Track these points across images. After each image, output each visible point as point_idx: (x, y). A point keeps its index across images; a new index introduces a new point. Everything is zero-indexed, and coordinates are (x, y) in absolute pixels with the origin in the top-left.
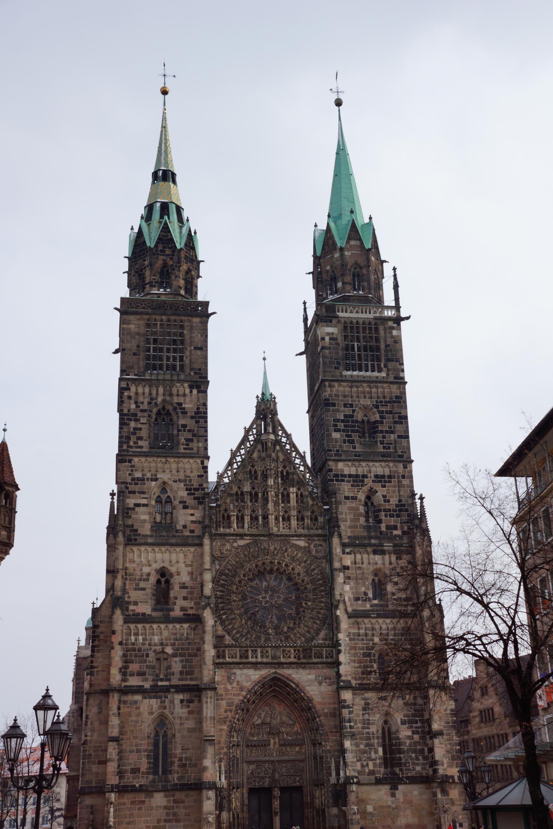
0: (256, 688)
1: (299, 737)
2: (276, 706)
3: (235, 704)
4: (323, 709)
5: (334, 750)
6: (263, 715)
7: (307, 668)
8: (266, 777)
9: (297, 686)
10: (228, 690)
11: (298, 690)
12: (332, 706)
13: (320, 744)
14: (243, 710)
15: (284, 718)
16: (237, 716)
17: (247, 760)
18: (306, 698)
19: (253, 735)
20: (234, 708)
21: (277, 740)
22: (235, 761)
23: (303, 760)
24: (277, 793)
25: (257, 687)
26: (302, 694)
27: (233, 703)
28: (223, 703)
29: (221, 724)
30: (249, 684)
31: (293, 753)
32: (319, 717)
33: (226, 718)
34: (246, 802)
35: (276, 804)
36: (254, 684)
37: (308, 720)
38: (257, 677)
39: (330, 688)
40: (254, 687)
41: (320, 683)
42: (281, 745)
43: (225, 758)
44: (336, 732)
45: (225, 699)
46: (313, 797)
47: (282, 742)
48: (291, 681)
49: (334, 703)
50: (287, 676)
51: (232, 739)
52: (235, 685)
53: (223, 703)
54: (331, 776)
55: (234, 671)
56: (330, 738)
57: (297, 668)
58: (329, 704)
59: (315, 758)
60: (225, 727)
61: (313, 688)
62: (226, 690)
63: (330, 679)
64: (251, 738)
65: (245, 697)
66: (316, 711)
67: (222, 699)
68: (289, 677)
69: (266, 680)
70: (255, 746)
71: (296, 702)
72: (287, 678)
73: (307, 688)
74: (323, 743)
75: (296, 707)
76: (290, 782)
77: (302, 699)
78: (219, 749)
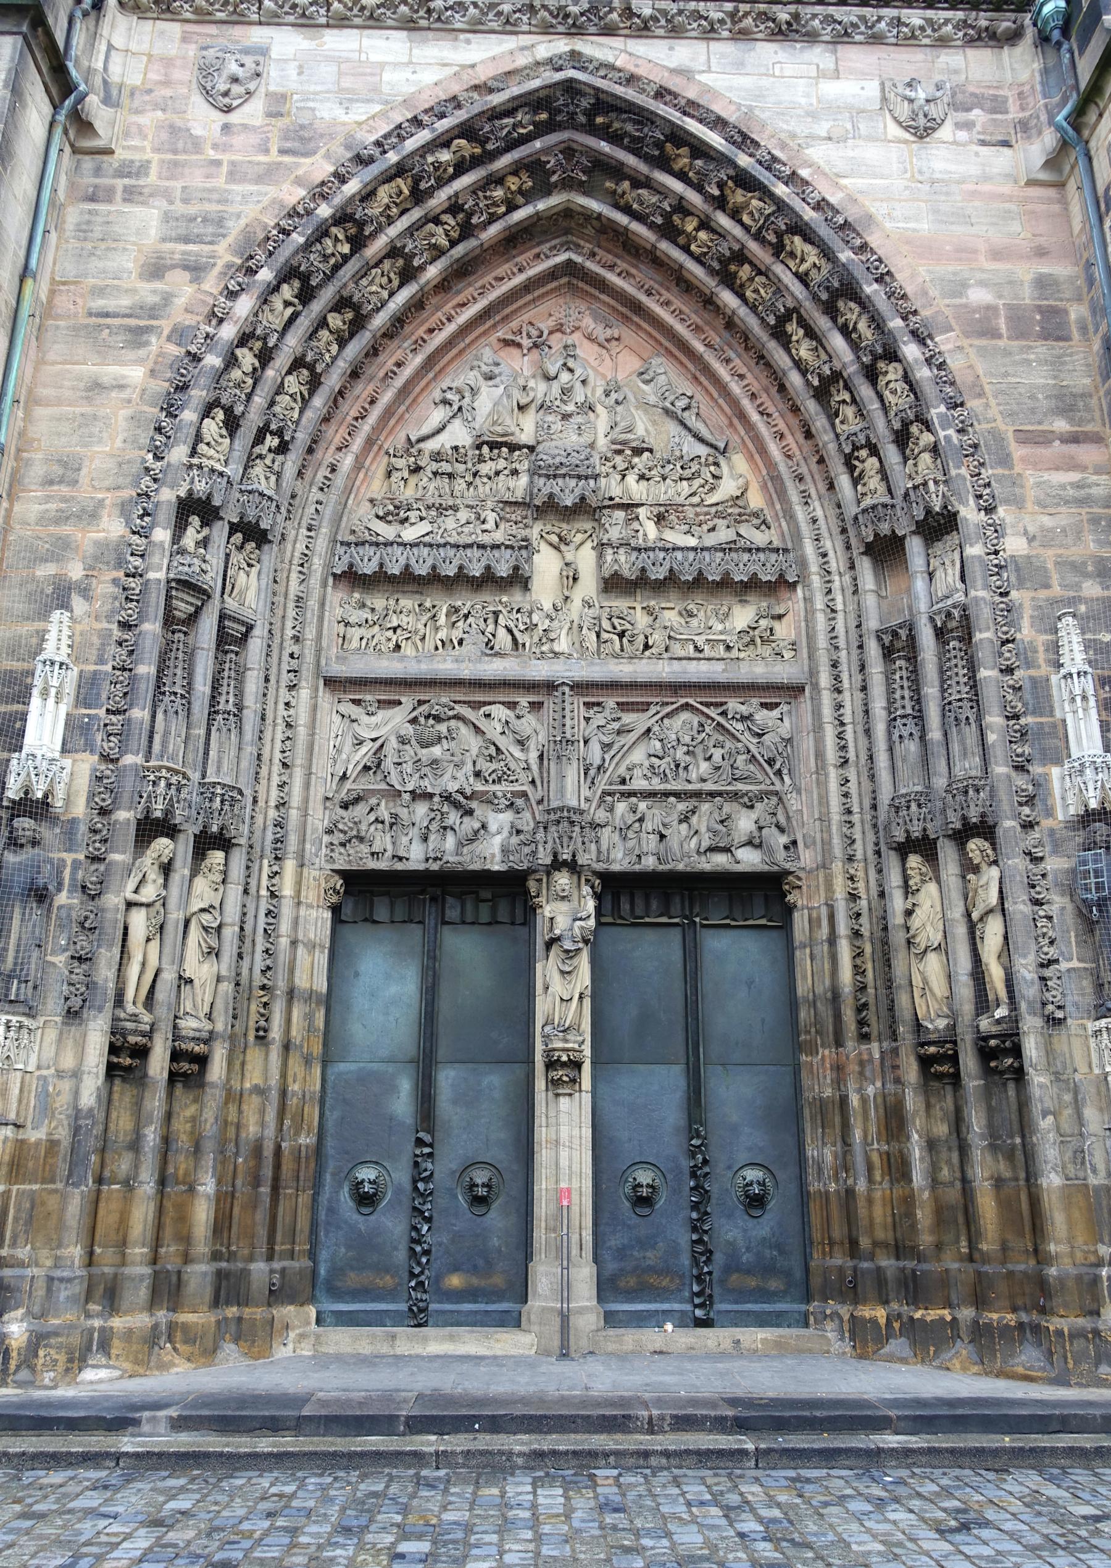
0: (411, 144)
1: (760, 538)
2: (586, 351)
3: (235, 229)
4: (960, 287)
5: (1077, 568)
6: (487, 400)
7: (812, 37)
8: (489, 800)
9: (744, 140)
10: (197, 145)
11: (744, 160)
12: (1026, 272)
13: (939, 526)
14: (306, 295)
15: (643, 427)
16: (244, 306)
17: (338, 670)
18: (808, 214)
19: (397, 514)
20: (224, 254)
21: (585, 559)
22: (208, 626)
23: (795, 690)
24: (566, 910)
25: (423, 136)
26: (781, 190)
27: (220, 222)
28: (144, 224)
29: (103, 351)
30: (360, 112)
31: (707, 639)
32: (919, 338)
33: (153, 312)
34: (311, 971)
35: (562, 993)
36: (400, 116)
37: (821, 394)
38: (429, 77)
39: (1001, 160)
40: (399, 133)
41: (922, 129)
42: (613, 584)
43: (104, 587)
44: (1074, 439)
45: (167, 195)
46: (883, 946)
47: (625, 563)
48: (690, 108)
49: (1041, 253)
50: (660, 78)
51: (179, 454)
52: (252, 112)
53: (144, 224)
54: (1058, 754)
55: (257, 35)
56: (1031, 477)
57: (742, 35)
58: (996, 254)
59: (898, 645)
60: (136, 374)
61: (872, 153)
62: (177, 138)
63: (997, 106)
64: (387, 531)
65: (321, 193)
66: (897, 296)
67: (131, 195)
68: (674, 83)
69: (496, 99)
70: (408, 581)
71: (728, 280)
72: (662, 93)
73: (817, 153)
74: (969, 513)
75: (730, 324)
76: (687, 847)
77: (786, 230)
78: (61, 518)
